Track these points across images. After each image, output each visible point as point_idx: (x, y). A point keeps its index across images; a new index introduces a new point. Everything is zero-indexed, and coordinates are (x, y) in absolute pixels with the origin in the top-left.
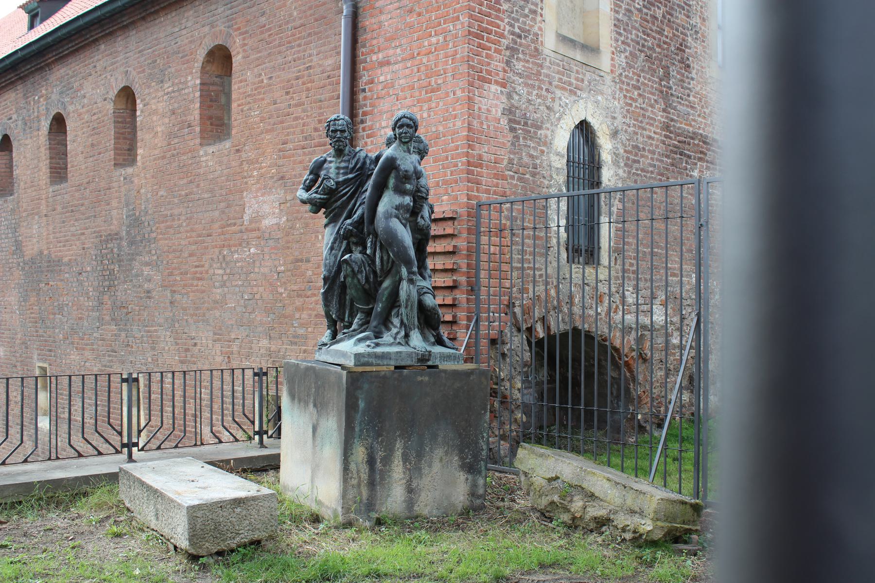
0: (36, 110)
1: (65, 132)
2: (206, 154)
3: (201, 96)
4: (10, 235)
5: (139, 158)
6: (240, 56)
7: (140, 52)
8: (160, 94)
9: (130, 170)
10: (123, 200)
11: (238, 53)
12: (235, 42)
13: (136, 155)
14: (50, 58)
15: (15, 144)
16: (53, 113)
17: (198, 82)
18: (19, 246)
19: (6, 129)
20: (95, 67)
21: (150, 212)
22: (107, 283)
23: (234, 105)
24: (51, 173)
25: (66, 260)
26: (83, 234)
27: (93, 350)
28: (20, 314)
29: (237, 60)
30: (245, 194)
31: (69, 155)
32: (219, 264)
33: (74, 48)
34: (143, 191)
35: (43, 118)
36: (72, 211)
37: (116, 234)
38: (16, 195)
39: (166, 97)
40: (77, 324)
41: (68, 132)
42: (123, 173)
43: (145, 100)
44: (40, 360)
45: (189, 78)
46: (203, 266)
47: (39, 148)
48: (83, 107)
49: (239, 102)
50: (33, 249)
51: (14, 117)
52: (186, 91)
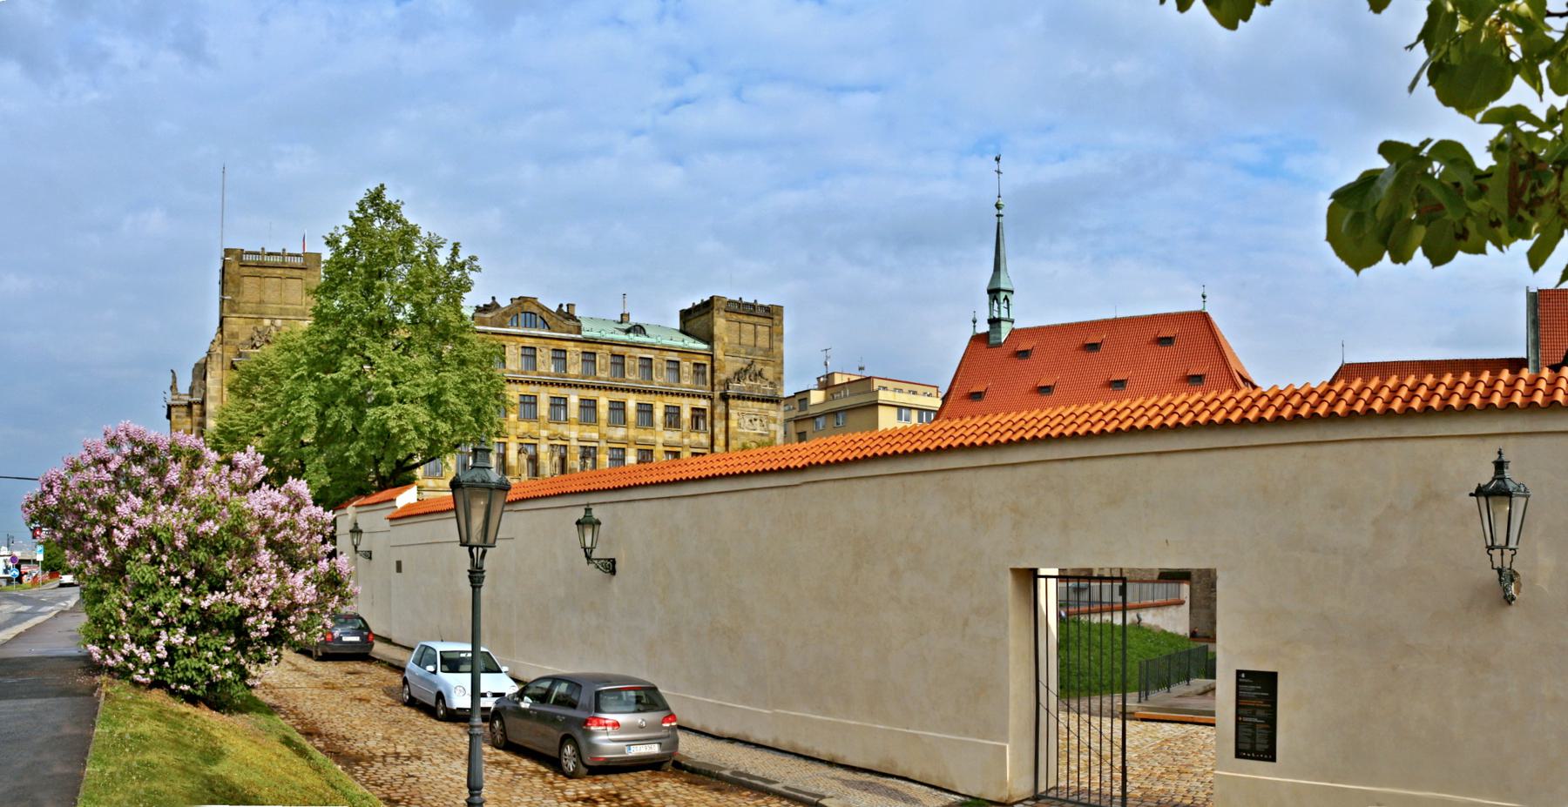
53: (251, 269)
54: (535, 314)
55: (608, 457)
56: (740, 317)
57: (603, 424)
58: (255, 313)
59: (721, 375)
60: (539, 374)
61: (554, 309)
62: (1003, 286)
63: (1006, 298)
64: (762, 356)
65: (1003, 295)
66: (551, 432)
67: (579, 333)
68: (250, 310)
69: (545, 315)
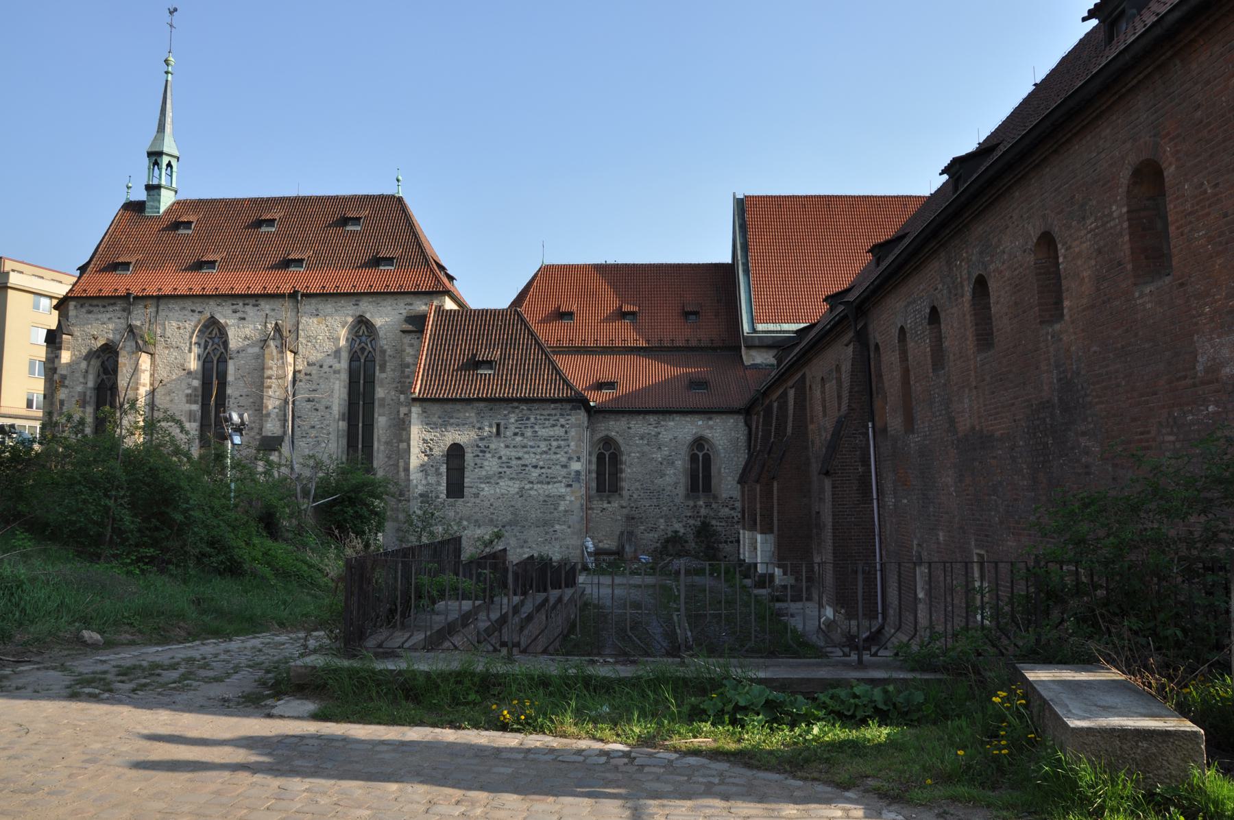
0: (959, 276)
1: (988, 295)
2: (1141, 296)
3: (1130, 226)
4: (944, 412)
5: (1066, 311)
6: (1173, 168)
7: (1055, 191)
8: (1083, 233)
9: (1057, 327)
10: (1052, 361)
11: (1170, 164)
12: (1165, 151)
13: (1062, 309)
14: (966, 218)
15: (942, 315)
16: (975, 276)
17: (1124, 210)
18: (952, 421)
19: (933, 301)
20: (1011, 217)
21: (1083, 372)
22: (1042, 458)
23: (1172, 229)
24: (977, 340)
25: (997, 434)
26: (1013, 404)
27: (1030, 535)
28: (957, 496)
29: (1170, 172)
30: (1196, 337)
31: (994, 319)
32: (1169, 430)
33: (988, 202)
34: (1073, 348)
35: (966, 283)
36: (1001, 380)
37: (1048, 402)
38: (947, 369)
39: (1089, 235)
40: (1012, 506)
41: (991, 294)
42: (1050, 330)
43: (1066, 243)
44: (977, 546)
45: (1114, 208)
46: (1148, 432)
47: (964, 315)
48: (1003, 263)
49: (1178, 224)
50: (965, 425)
51: (940, 286)
52: (1112, 224)
62: (166, 150)
63: (169, 165)
65: (165, 160)
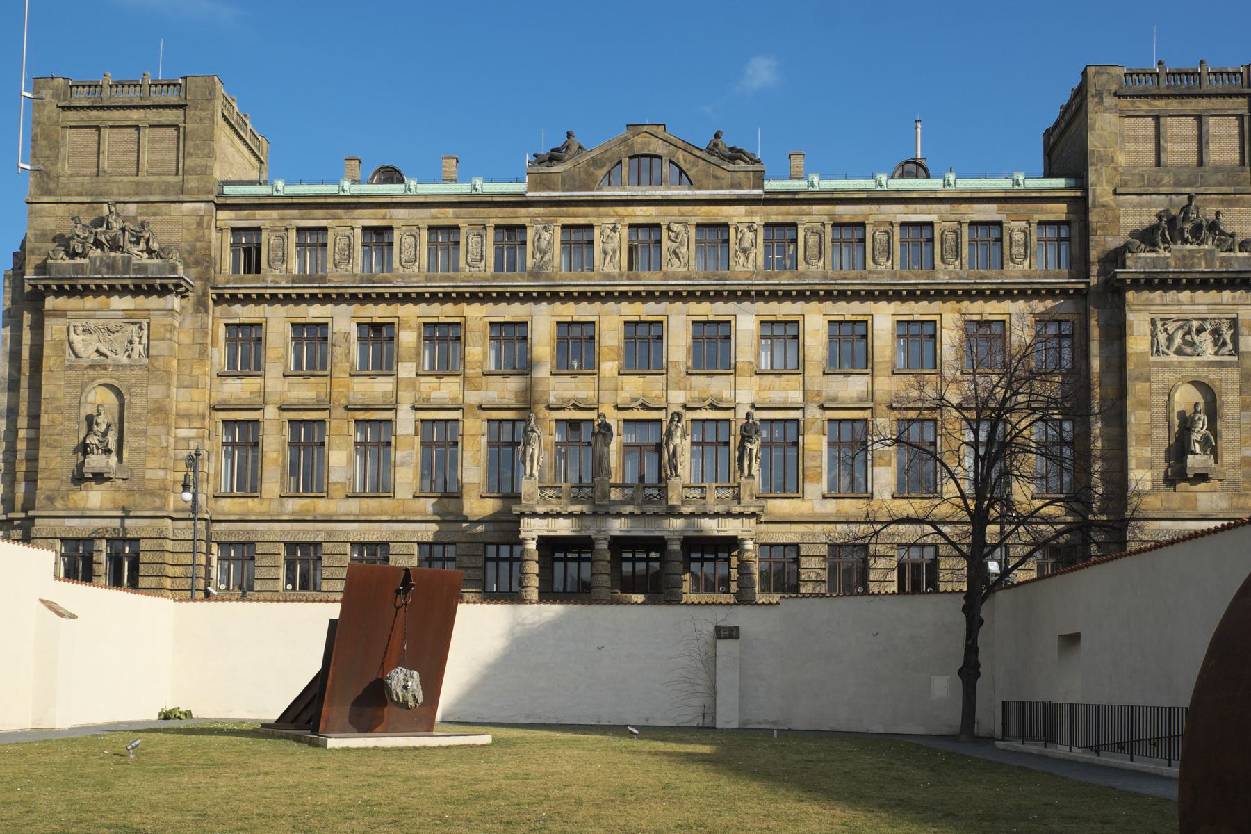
53: (83, 115)
54: (660, 157)
55: (825, 440)
56: (1160, 104)
57: (814, 371)
58: (87, 194)
59: (1109, 239)
60: (666, 276)
61: (704, 142)
64: (1221, 185)
66: (695, 394)
67: (761, 186)
68: (79, 189)
69: (680, 156)
